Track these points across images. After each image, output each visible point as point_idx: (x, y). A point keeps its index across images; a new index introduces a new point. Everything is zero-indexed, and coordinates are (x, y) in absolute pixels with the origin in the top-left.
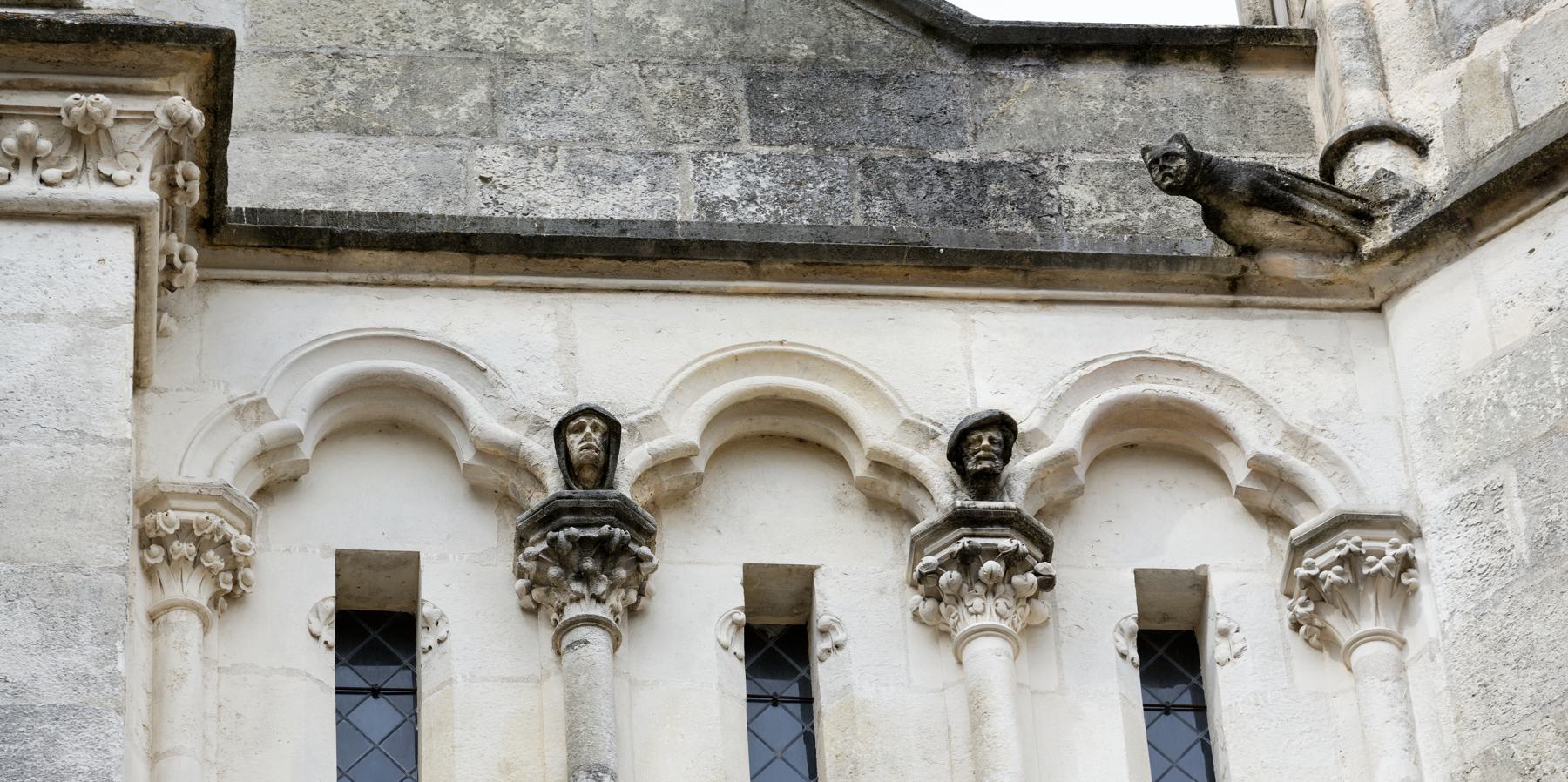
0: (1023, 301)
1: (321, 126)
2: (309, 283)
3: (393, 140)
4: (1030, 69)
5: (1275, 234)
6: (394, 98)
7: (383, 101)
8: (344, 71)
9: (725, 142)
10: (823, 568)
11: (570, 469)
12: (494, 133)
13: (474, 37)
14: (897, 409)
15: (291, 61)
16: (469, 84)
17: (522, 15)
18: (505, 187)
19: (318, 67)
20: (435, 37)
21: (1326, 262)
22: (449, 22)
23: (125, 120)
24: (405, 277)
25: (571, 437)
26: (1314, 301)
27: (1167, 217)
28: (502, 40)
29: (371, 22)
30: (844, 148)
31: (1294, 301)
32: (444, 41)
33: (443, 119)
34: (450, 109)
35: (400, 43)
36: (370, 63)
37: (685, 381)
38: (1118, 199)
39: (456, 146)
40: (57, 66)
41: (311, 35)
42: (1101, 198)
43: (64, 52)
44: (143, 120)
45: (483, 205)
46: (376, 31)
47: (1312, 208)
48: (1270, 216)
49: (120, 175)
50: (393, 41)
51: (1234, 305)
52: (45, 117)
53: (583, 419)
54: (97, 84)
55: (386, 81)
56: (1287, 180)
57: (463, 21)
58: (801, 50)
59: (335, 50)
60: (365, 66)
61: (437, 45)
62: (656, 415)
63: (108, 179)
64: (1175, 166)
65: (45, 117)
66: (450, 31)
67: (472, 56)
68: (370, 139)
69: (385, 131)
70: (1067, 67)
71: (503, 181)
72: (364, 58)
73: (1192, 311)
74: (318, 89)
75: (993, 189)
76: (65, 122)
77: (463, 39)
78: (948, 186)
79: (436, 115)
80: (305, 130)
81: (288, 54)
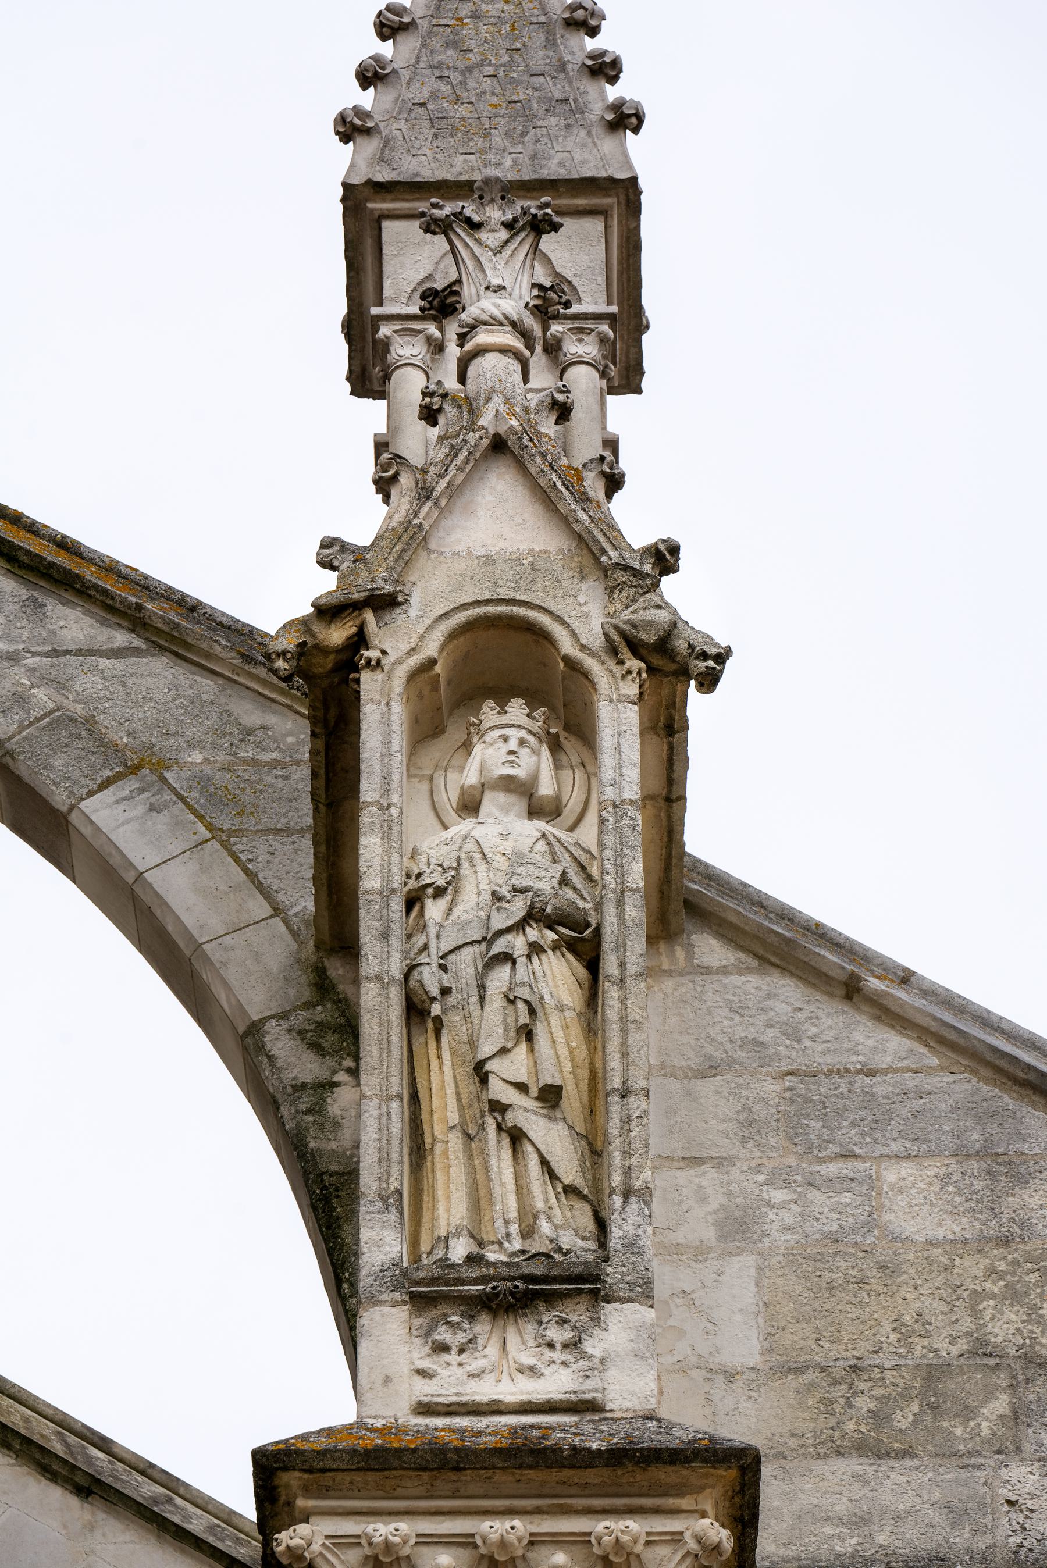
1: (842, 1450)
3: (915, 1463)
6: (915, 1414)
7: (903, 1419)
8: (862, 1386)
12: (1018, 1449)
13: (993, 1340)
15: (807, 1377)
16: (990, 1395)
17: (1041, 1312)
18: (1032, 1511)
19: (836, 1382)
20: (953, 1343)
22: (967, 1323)
23: (655, 1541)
28: (1022, 1341)
29: (887, 1327)
32: (963, 1345)
33: (966, 1436)
34: (972, 1424)
35: (918, 1351)
36: (889, 1374)
39: (979, 1467)
40: (586, 1490)
41: (827, 1345)
43: (592, 1476)
44: (673, 1540)
45: (1010, 1533)
46: (893, 1337)
50: (910, 1348)
52: (575, 1542)
54: (625, 1505)
55: (906, 1396)
57: (981, 1322)
59: (853, 1362)
60: (883, 1378)
61: (955, 1351)
65: (575, 1542)
66: (968, 1334)
67: (992, 1361)
68: (892, 1463)
69: (907, 1453)
71: (1030, 1504)
72: (882, 1369)
74: (837, 1408)
76: (596, 1550)
77: (983, 1343)
79: (958, 1432)
80: (826, 1456)
81: (804, 1369)
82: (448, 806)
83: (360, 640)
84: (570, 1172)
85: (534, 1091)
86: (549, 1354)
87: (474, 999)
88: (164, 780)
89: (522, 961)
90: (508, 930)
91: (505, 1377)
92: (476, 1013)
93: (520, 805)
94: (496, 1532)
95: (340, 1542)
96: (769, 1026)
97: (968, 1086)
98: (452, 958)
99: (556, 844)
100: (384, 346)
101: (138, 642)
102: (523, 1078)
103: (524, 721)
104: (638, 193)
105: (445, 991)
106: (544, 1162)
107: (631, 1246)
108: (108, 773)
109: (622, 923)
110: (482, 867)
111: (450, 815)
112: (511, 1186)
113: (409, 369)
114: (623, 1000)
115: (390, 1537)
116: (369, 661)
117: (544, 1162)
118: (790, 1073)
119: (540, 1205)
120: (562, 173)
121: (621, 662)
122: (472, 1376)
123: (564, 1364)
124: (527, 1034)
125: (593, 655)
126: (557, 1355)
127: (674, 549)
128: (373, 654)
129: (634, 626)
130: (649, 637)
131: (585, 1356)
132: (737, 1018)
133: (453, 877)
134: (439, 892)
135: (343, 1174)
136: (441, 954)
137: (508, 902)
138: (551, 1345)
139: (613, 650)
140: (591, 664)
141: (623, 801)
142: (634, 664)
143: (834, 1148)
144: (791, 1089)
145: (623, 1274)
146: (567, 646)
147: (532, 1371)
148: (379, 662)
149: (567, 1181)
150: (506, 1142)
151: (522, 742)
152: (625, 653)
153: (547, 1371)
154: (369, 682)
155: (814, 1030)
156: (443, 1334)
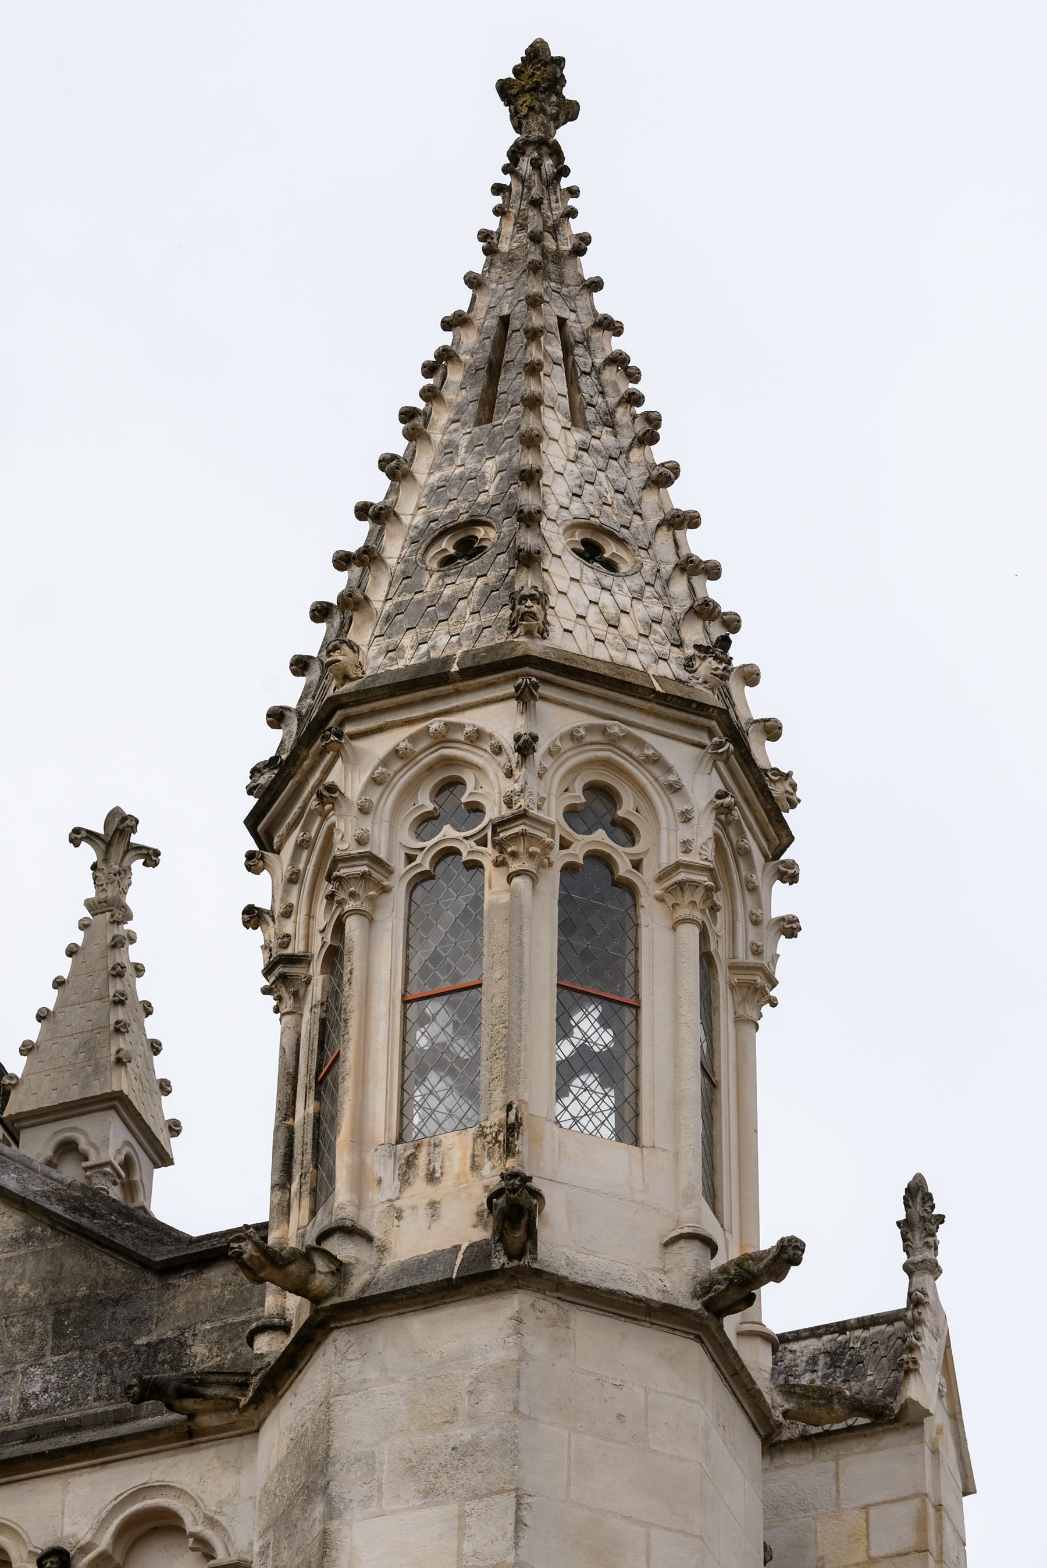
0: (94, 1466)
4: (189, 1276)
5: (197, 1407)
9: (38, 1359)
21: (225, 1415)
26: (227, 1434)
27: (240, 1354)
30: (93, 1349)
31: (219, 1436)
38: (218, 1348)
42: (210, 1350)
47: (210, 1391)
48: (192, 1400)
51: (191, 1445)
56: (197, 1379)
58: (83, 1291)
64: (132, 1392)
70: (206, 1271)
73: (172, 1452)
75: (161, 1356)
78: (139, 1360)
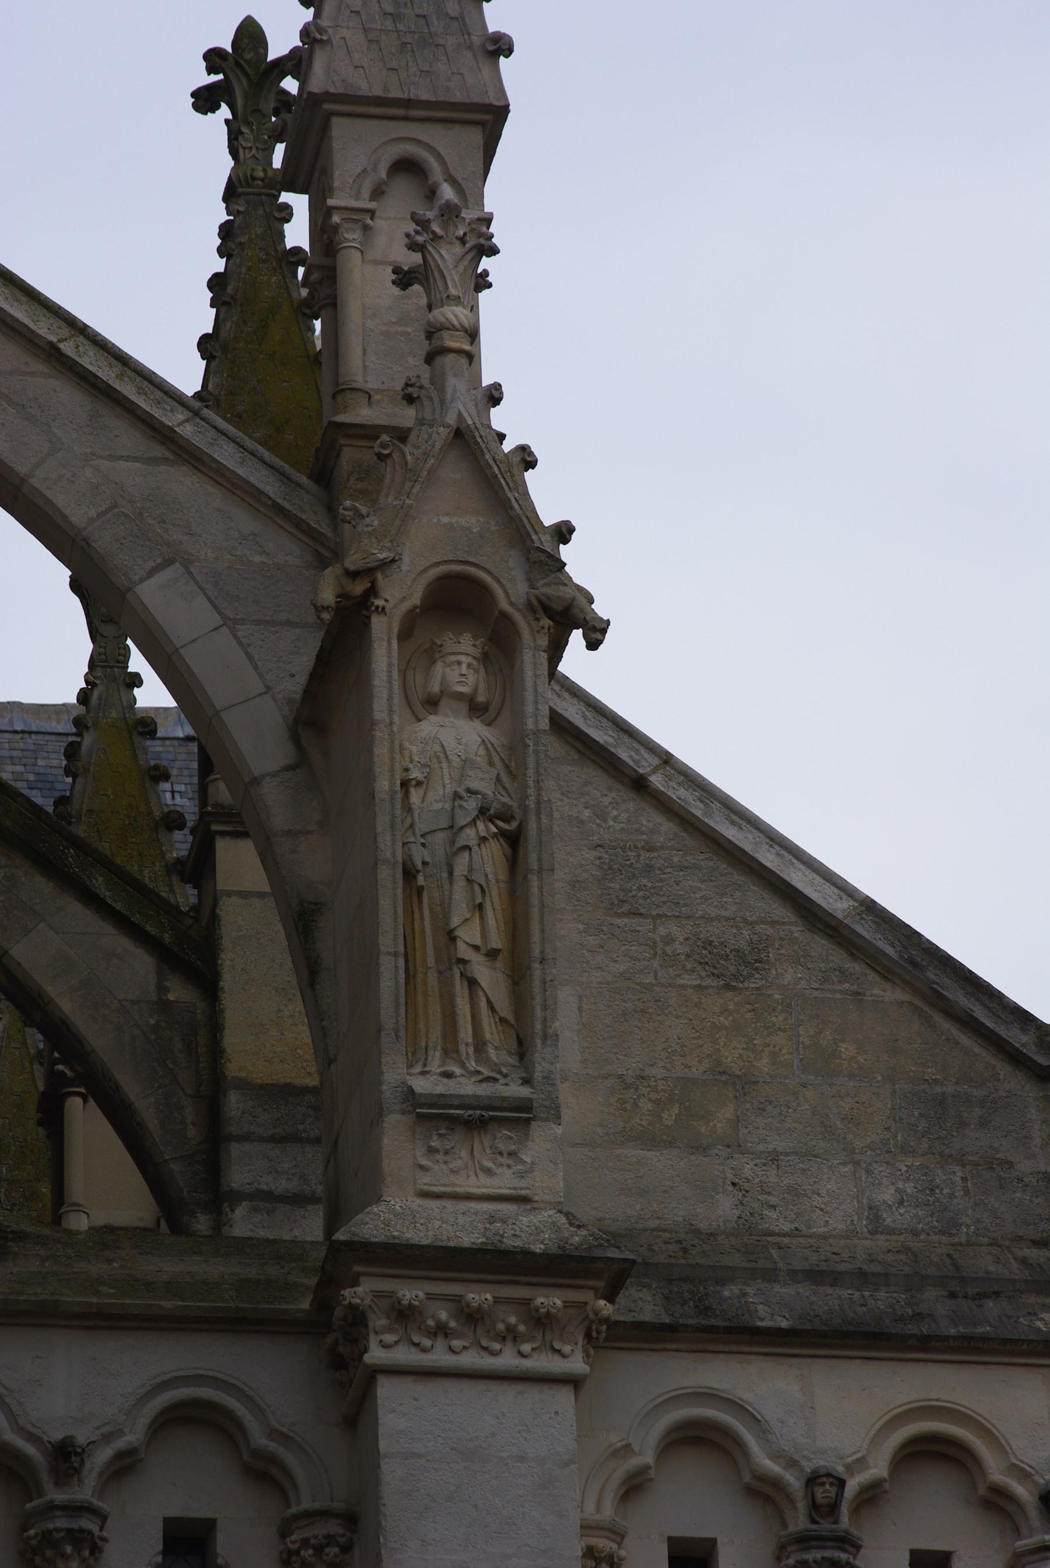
2: (653, 1350)
6: (676, 1115)
8: (645, 1091)
10: (957, 1553)
11: (814, 1506)
13: (725, 1061)
14: (1007, 1454)
17: (755, 1042)
18: (747, 1191)
19: (627, 1087)
20: (700, 1062)
24: (711, 1347)
25: (816, 1488)
28: (743, 1064)
33: (708, 1133)
34: (711, 1124)
37: (880, 1430)
41: (621, 1057)
44: (577, 1307)
45: (734, 1207)
49: (567, 1349)
52: (519, 1303)
53: (824, 1480)
57: (718, 1047)
60: (656, 1086)
62: (863, 1457)
63: (559, 1351)
65: (519, 1303)
66: (709, 1056)
67: (724, 1078)
77: (719, 1063)
79: (703, 1130)
82: (418, 702)
83: (372, 591)
84: (505, 1009)
85: (483, 951)
86: (500, 1159)
87: (445, 875)
88: (190, 573)
89: (475, 848)
90: (467, 825)
91: (472, 1174)
92: (447, 886)
93: (464, 707)
94: (476, 1302)
95: (378, 1295)
96: (586, 807)
97: (711, 864)
98: (429, 837)
99: (491, 749)
100: (336, 228)
101: (168, 454)
102: (478, 941)
103: (470, 650)
104: (508, 112)
105: (425, 863)
106: (489, 1002)
107: (548, 1078)
108: (151, 564)
109: (539, 828)
110: (445, 765)
111: (420, 709)
112: (469, 1018)
113: (353, 251)
114: (541, 888)
115: (413, 1301)
116: (377, 607)
117: (489, 1002)
118: (599, 846)
119: (488, 1036)
120: (458, 97)
121: (538, 619)
122: (452, 1171)
123: (509, 1166)
124: (480, 907)
125: (518, 610)
126: (504, 1160)
127: (571, 530)
128: (379, 602)
129: (549, 598)
130: (558, 607)
131: (522, 1162)
132: (566, 800)
133: (428, 773)
134: (419, 784)
135: (316, 904)
136: (422, 833)
137: (466, 801)
138: (501, 1154)
139: (530, 607)
140: (517, 616)
141: (538, 731)
142: (546, 622)
143: (626, 908)
144: (600, 858)
145: (543, 1099)
146: (504, 605)
147: (488, 1172)
148: (384, 608)
149: (502, 1015)
150: (466, 984)
151: (469, 665)
152: (541, 613)
153: (498, 1171)
154: (377, 624)
155: (615, 813)
156: (435, 1143)
